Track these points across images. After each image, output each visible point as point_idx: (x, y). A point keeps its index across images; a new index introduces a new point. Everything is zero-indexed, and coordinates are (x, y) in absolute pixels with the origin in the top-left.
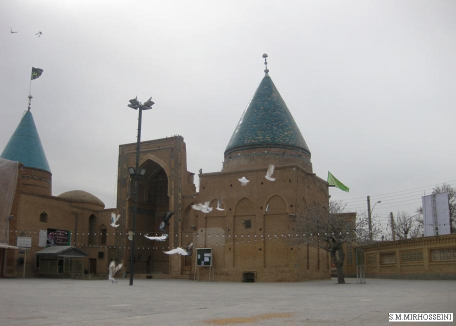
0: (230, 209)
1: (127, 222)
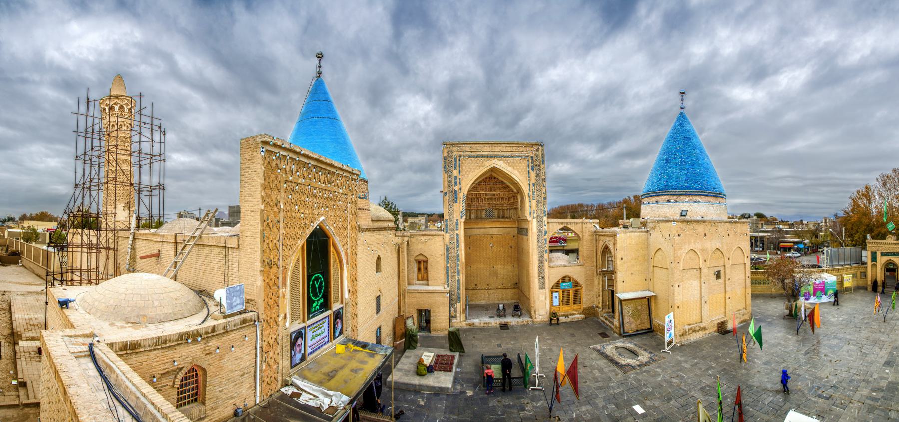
0: (705, 260)
1: (463, 252)
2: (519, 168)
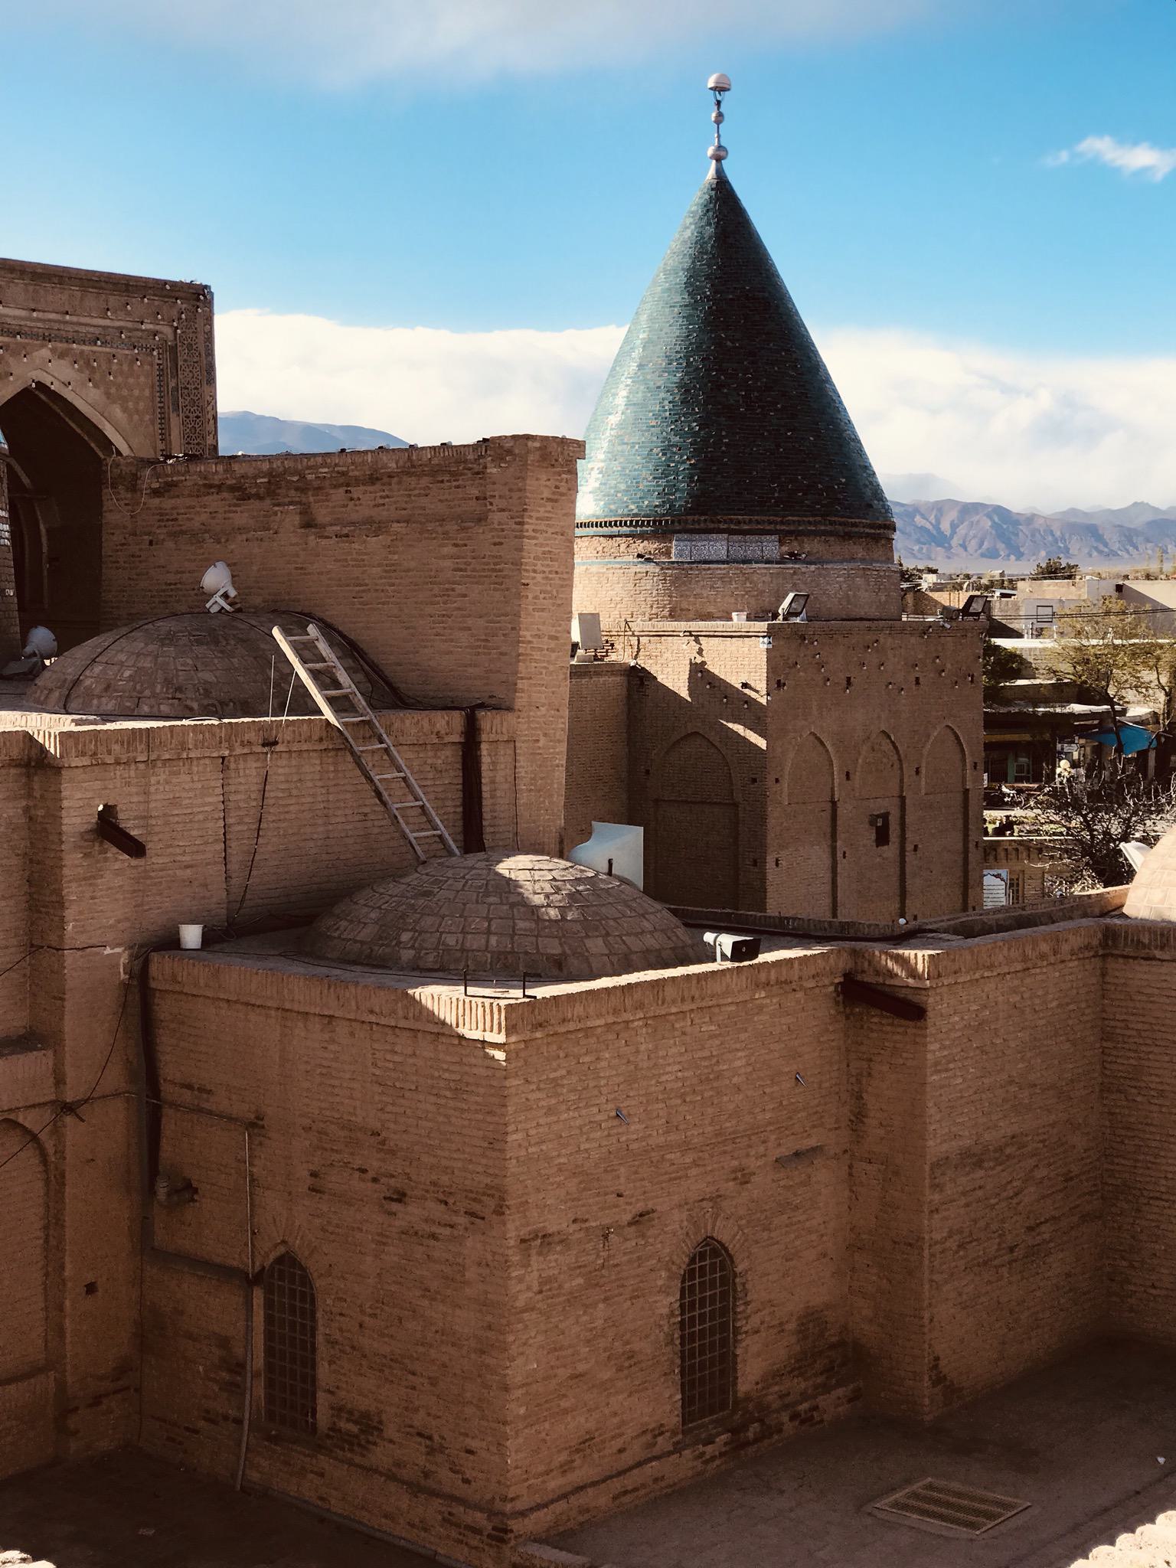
0: (848, 774)
2: (125, 392)
